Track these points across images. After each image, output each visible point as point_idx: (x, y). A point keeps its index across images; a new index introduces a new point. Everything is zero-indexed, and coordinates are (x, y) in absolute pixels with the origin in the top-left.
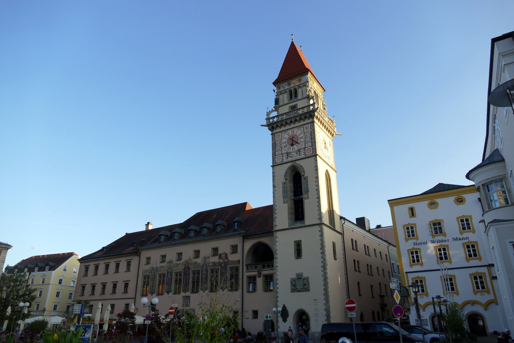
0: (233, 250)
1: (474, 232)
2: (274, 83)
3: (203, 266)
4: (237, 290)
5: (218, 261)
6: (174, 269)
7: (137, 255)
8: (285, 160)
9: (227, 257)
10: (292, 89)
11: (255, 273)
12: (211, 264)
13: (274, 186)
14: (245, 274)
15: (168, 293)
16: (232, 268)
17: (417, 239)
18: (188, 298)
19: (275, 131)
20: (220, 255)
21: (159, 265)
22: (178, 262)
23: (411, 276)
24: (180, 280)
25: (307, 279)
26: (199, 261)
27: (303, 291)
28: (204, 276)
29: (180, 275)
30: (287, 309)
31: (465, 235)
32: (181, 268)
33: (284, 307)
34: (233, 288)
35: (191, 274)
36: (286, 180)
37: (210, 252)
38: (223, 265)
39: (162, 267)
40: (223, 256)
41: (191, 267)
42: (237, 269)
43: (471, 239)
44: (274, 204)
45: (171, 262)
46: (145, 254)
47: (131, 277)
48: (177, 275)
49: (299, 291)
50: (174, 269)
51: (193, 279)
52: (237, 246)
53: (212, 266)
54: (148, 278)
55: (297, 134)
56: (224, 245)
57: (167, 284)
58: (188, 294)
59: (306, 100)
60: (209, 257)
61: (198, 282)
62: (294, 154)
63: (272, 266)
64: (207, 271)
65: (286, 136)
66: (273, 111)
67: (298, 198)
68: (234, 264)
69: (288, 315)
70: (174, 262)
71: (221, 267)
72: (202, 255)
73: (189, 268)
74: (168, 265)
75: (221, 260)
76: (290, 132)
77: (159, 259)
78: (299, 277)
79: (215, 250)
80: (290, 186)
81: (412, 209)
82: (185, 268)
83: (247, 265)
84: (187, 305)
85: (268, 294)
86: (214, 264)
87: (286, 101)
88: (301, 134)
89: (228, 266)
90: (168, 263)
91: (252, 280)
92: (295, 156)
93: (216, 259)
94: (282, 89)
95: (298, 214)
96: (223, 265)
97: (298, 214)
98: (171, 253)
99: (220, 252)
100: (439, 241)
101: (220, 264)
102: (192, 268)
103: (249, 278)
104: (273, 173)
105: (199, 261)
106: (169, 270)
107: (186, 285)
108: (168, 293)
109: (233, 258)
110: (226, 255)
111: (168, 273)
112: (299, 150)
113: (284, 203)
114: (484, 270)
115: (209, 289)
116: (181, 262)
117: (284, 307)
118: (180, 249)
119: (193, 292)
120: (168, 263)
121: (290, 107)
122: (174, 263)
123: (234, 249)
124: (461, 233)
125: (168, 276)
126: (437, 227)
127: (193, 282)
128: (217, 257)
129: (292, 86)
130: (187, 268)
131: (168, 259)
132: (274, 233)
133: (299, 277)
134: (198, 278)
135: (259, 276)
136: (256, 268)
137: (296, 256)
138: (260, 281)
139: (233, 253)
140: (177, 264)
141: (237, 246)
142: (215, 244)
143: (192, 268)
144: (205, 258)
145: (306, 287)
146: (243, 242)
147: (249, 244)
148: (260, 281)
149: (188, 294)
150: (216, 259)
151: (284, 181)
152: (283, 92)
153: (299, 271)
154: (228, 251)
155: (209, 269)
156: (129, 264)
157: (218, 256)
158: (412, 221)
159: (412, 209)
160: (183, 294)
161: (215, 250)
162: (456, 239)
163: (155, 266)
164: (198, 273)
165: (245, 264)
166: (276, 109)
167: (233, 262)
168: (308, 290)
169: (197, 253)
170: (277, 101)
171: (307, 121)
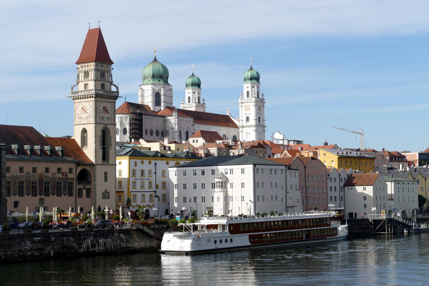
1: (152, 177)
3: (52, 179)
4: (73, 196)
5: (61, 177)
9: (67, 175)
11: (82, 187)
12: (57, 178)
13: (96, 137)
14: (76, 186)
15: (28, 195)
16: (69, 183)
17: (136, 177)
18: (43, 199)
20: (63, 173)
21: (19, 174)
22: (34, 174)
23: (132, 193)
25: (109, 192)
26: (49, 175)
28: (53, 186)
29: (36, 183)
31: (150, 178)
32: (36, 179)
33: (99, 206)
34: (71, 194)
39: (21, 176)
40: (65, 174)
41: (44, 178)
42: (72, 183)
43: (151, 180)
45: (28, 173)
48: (33, 183)
55: (108, 107)
56: (65, 167)
59: (109, 84)
61: (48, 189)
62: (106, 119)
64: (55, 183)
65: (102, 105)
71: (64, 181)
73: (42, 179)
74: (26, 175)
75: (63, 177)
76: (104, 103)
78: (106, 191)
79: (59, 170)
81: (136, 162)
85: (88, 199)
86: (59, 178)
88: (109, 108)
90: (26, 173)
91: (80, 191)
92: (106, 122)
93: (60, 175)
94: (98, 68)
99: (63, 171)
100: (143, 179)
101: (63, 179)
102: (45, 180)
103: (79, 189)
104: (95, 128)
105: (49, 175)
106: (28, 179)
108: (28, 195)
109: (70, 176)
110: (67, 173)
112: (108, 118)
114: (153, 193)
116: (37, 174)
117: (99, 206)
118: (35, 165)
119: (45, 195)
120: (26, 173)
123: (70, 170)
124: (149, 177)
126: (142, 172)
127: (45, 189)
128: (61, 174)
129: (103, 68)
130: (41, 179)
131: (25, 170)
133: (106, 191)
134: (48, 187)
135: (84, 189)
136: (82, 183)
138: (84, 192)
140: (34, 175)
143: (45, 180)
144: (54, 174)
146: (76, 167)
147: (79, 169)
148: (84, 192)
149: (43, 196)
150: (60, 175)
153: (106, 189)
154: (68, 172)
158: (135, 168)
159: (136, 162)
161: (59, 170)
162: (147, 179)
164: (48, 183)
167: (71, 179)
168: (109, 198)
169: (47, 170)
171: (112, 101)
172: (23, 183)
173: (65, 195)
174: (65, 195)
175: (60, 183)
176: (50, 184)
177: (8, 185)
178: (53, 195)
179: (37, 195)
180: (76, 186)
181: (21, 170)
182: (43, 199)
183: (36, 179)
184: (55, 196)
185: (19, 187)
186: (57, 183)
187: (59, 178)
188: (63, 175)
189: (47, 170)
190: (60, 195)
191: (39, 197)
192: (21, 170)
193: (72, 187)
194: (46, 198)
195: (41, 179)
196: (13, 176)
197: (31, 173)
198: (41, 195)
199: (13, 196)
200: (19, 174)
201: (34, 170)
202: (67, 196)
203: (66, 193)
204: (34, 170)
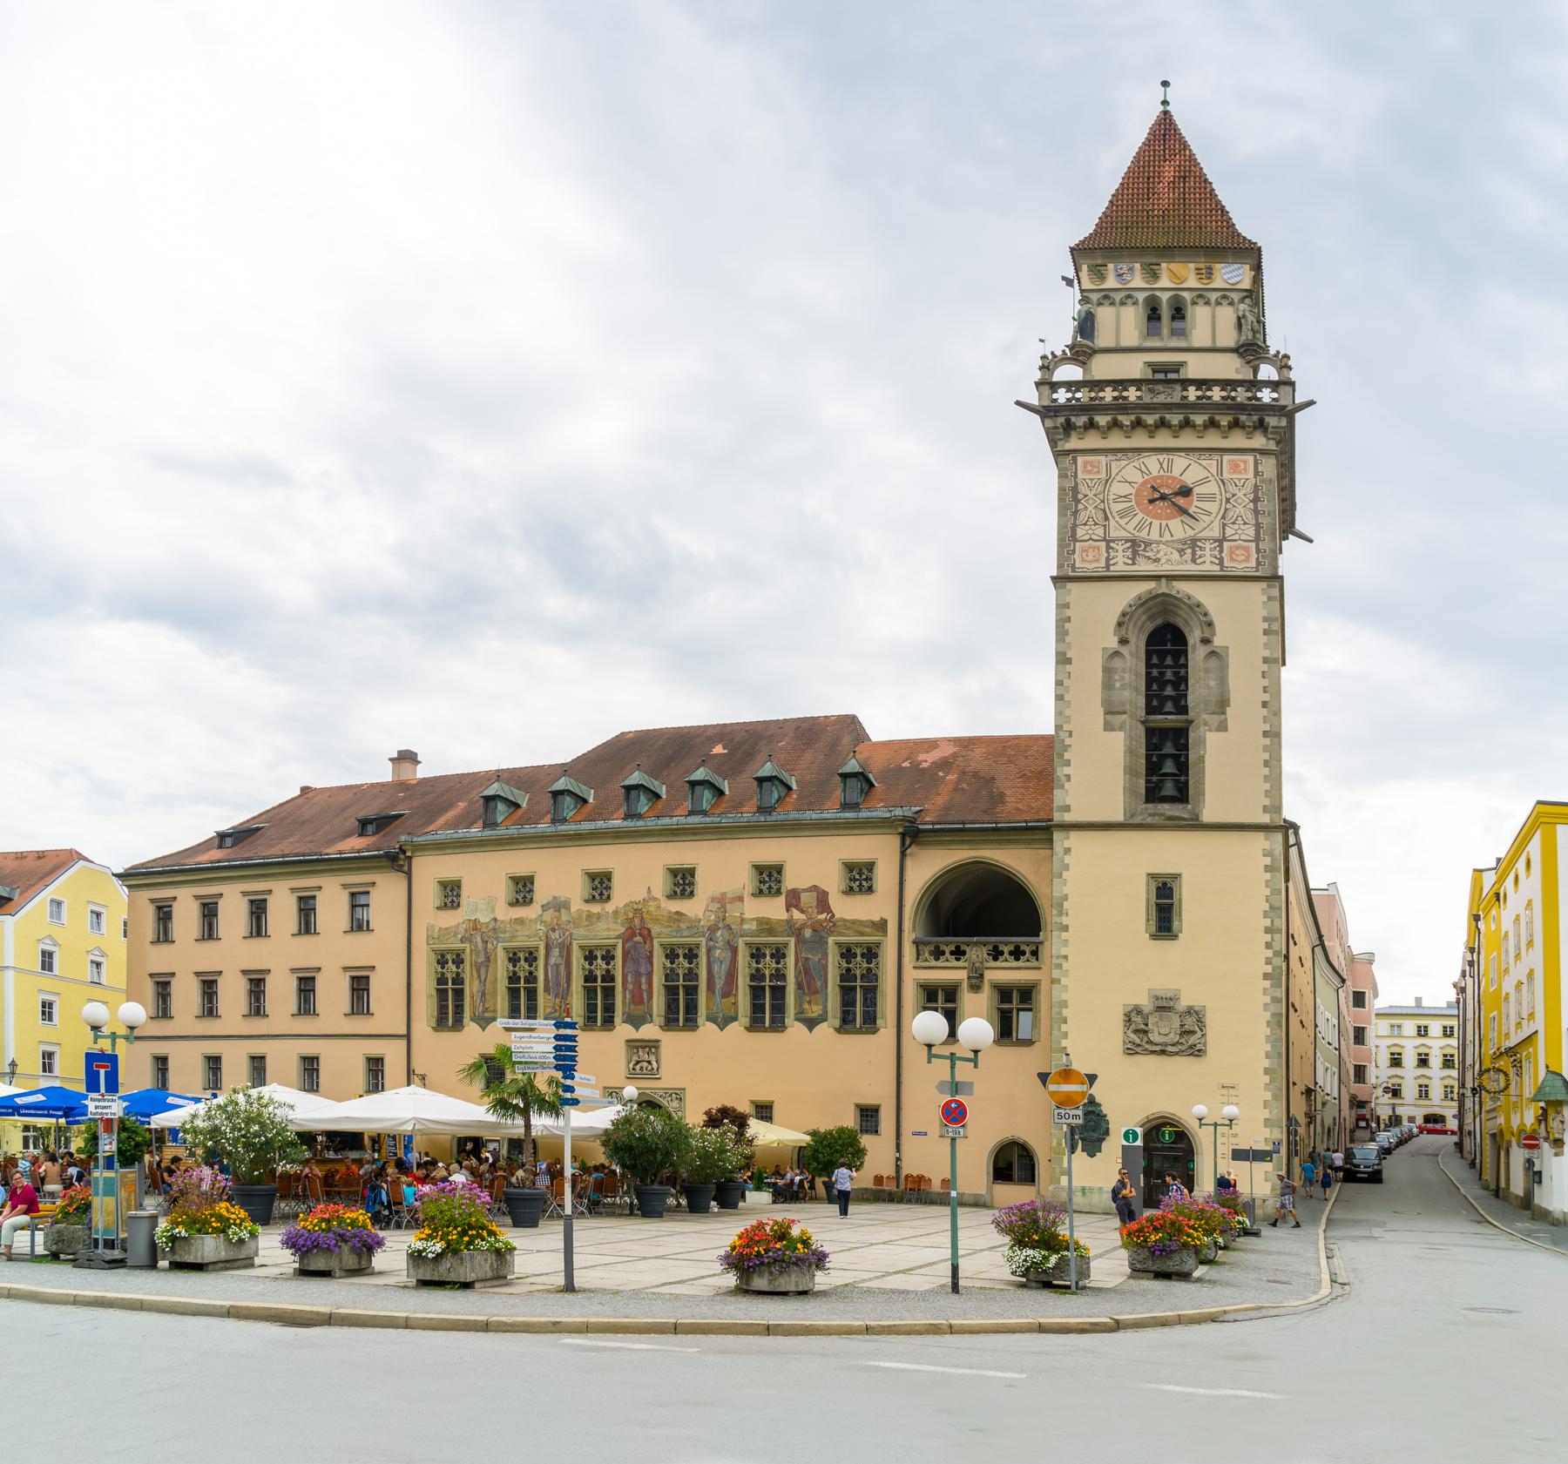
0: (853, 880)
2: (1079, 252)
3: (713, 929)
4: (875, 1031)
5: (784, 916)
6: (581, 931)
7: (399, 869)
8: (1121, 565)
10: (1165, 297)
14: (903, 969)
18: (652, 1046)
19: (1074, 443)
20: (793, 899)
21: (505, 913)
22: (595, 908)
24: (609, 977)
26: (694, 908)
27: (1177, 1054)
28: (720, 971)
29: (609, 958)
30: (1105, 1110)
35: (659, 959)
36: (1124, 641)
37: (744, 880)
38: (808, 933)
39: (520, 921)
40: (804, 897)
41: (655, 929)
42: (871, 953)
44: (1058, 727)
45: (559, 905)
46: (430, 870)
47: (381, 951)
48: (590, 957)
49: (1163, 1052)
50: (579, 932)
51: (670, 976)
52: (870, 866)
53: (759, 933)
54: (459, 961)
57: (547, 989)
58: (650, 1031)
60: (741, 899)
63: (1035, 953)
64: (734, 951)
66: (1064, 360)
67: (1170, 720)
68: (862, 934)
69: (1107, 1132)
70: (577, 905)
71: (800, 941)
72: (706, 886)
73: (647, 936)
74: (548, 916)
75: (797, 915)
77: (502, 891)
80: (1133, 665)
82: (628, 936)
83: (916, 943)
84: (653, 1075)
86: (766, 926)
87: (1131, 337)
89: (831, 940)
90: (545, 907)
93: (774, 909)
95: (1165, 777)
96: (808, 933)
97: (1165, 777)
98: (560, 873)
99: (790, 881)
101: (794, 929)
102: (662, 935)
107: (639, 998)
109: (848, 908)
111: (548, 948)
113: (1108, 727)
115: (744, 1019)
116: (610, 907)
119: (670, 1023)
121: (1149, 364)
122: (573, 909)
125: (552, 961)
127: (671, 991)
128: (781, 901)
131: (542, 893)
132: (1057, 836)
134: (692, 975)
137: (1153, 929)
139: (850, 891)
140: (590, 916)
141: (870, 866)
142: (768, 850)
143: (662, 935)
144: (722, 901)
145: (1192, 1040)
149: (650, 1031)
150: (774, 909)
151: (1113, 643)
152: (1118, 297)
154: (833, 882)
155: (741, 943)
156: (357, 901)
157: (782, 898)
160: (624, 1031)
163: (484, 918)
164: (691, 955)
165: (909, 937)
166: (1080, 353)
169: (682, 881)
170: (1086, 326)
172: (531, 958)
173: (811, 1024)
174: (811, 1024)
175: (779, 955)
176: (703, 959)
177: (523, 968)
178: (723, 1021)
179: (618, 1019)
180: (903, 969)
181: (523, 888)
182: (652, 1046)
183: (608, 931)
184: (736, 1029)
185: (514, 978)
186: (757, 955)
187: (760, 921)
188: (793, 899)
189: (682, 881)
190: (778, 1025)
191: (624, 1031)
192: (523, 888)
193: (871, 976)
194: (673, 1044)
195: (637, 932)
196: (475, 925)
197: (577, 905)
198: (636, 1021)
199: (471, 1027)
200: (505, 913)
201: (600, 884)
202: (823, 1028)
203: (814, 1010)
204: (600, 884)
